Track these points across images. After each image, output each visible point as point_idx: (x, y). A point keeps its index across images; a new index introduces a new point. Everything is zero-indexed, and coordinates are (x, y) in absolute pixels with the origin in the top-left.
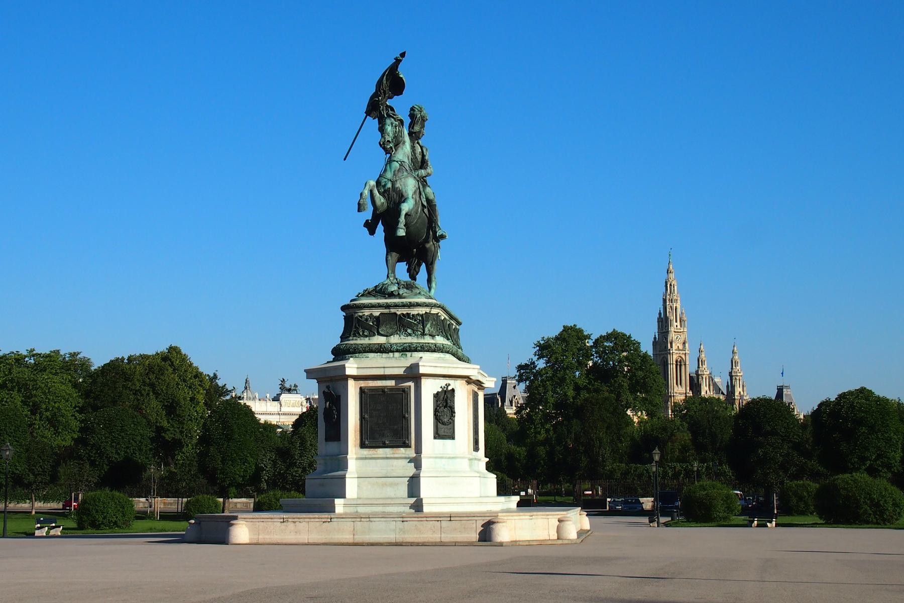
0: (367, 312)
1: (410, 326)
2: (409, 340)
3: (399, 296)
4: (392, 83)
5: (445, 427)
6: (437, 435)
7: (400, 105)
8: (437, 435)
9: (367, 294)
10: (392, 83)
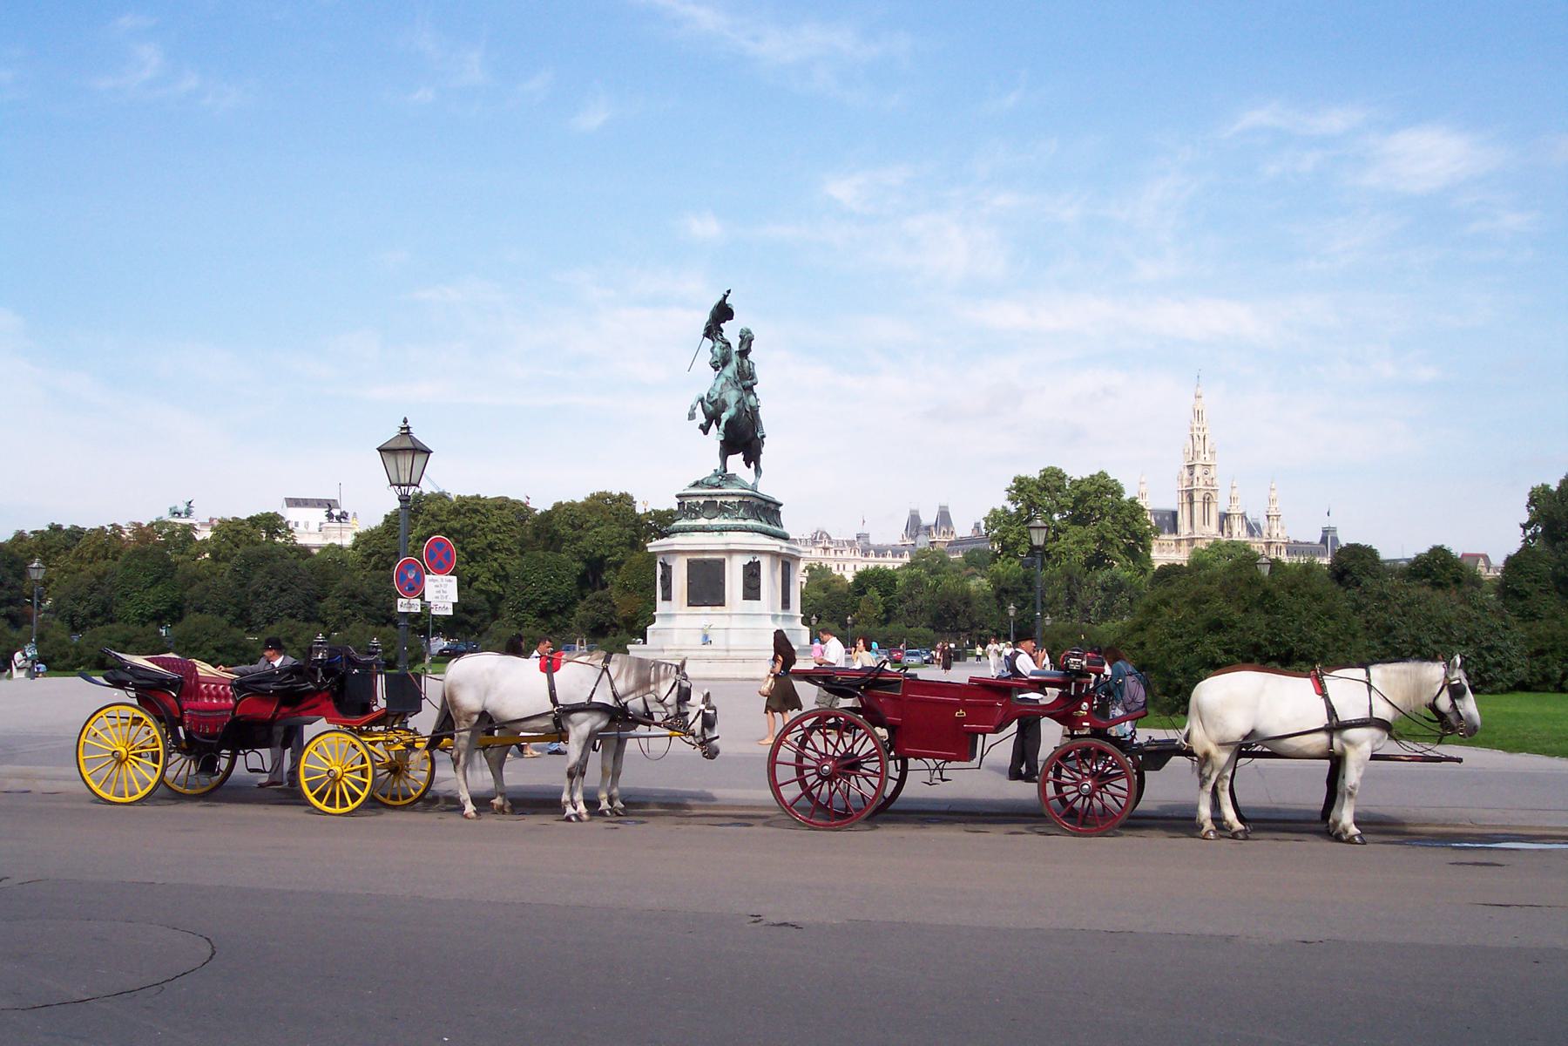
0: (694, 500)
1: (727, 510)
2: (725, 522)
3: (719, 487)
4: (723, 312)
5: (752, 590)
6: (746, 597)
7: (731, 331)
8: (746, 597)
9: (696, 484)
10: (723, 312)
